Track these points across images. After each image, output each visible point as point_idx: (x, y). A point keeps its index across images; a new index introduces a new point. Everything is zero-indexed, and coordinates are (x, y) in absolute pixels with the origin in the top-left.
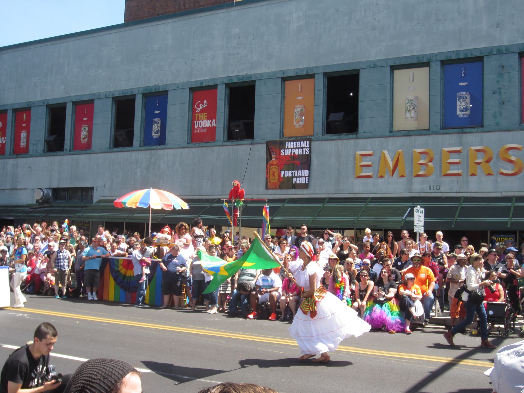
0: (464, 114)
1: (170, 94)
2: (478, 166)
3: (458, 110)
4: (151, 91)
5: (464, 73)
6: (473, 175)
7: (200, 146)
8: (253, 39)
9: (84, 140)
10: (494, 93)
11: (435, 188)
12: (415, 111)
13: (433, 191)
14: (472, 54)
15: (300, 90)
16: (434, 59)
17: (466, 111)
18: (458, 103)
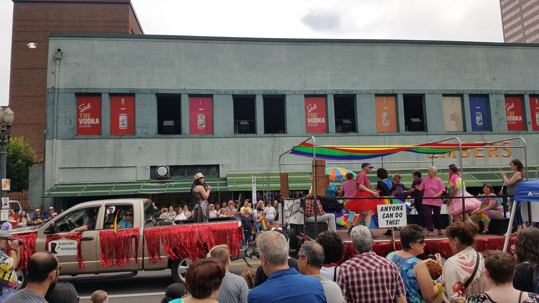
0: (480, 124)
1: (287, 97)
2: (492, 152)
3: (477, 122)
4: (270, 94)
5: (478, 102)
6: (490, 156)
7: (317, 136)
8: (353, 67)
9: (202, 126)
10: (496, 114)
11: (472, 164)
12: (455, 121)
13: (472, 165)
14: (484, 93)
15: (385, 103)
16: (465, 93)
17: (481, 122)
18: (477, 118)
